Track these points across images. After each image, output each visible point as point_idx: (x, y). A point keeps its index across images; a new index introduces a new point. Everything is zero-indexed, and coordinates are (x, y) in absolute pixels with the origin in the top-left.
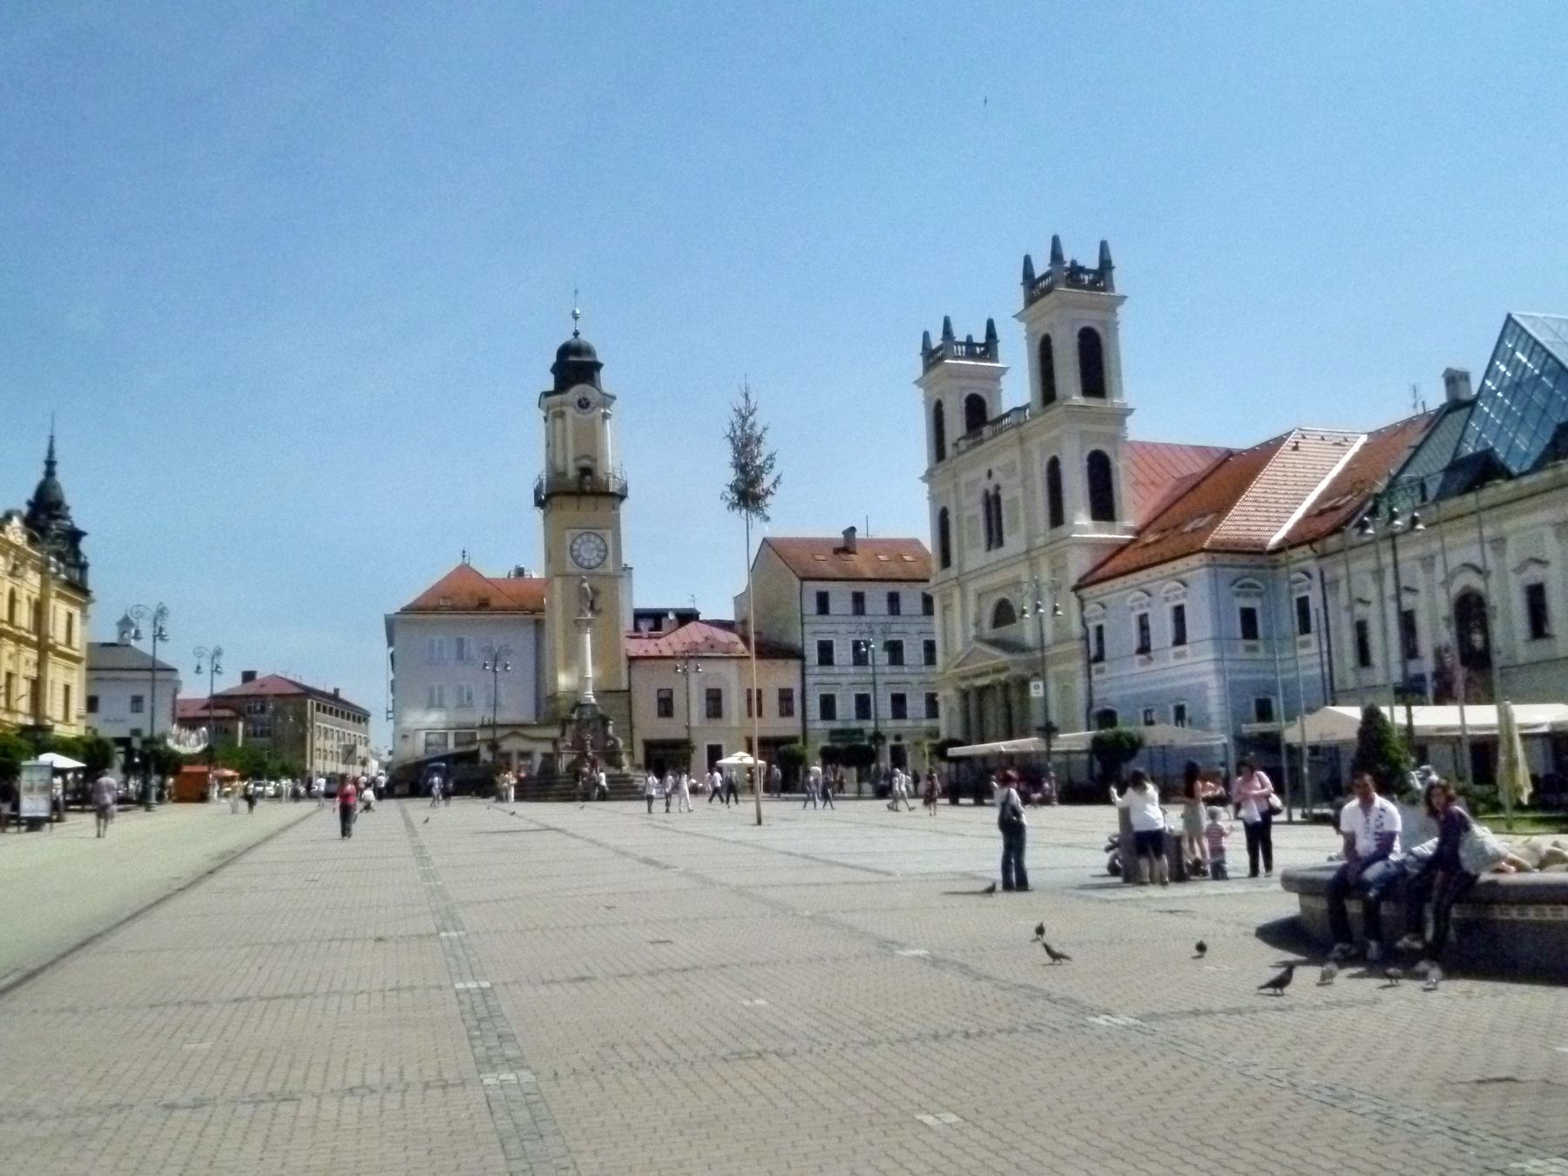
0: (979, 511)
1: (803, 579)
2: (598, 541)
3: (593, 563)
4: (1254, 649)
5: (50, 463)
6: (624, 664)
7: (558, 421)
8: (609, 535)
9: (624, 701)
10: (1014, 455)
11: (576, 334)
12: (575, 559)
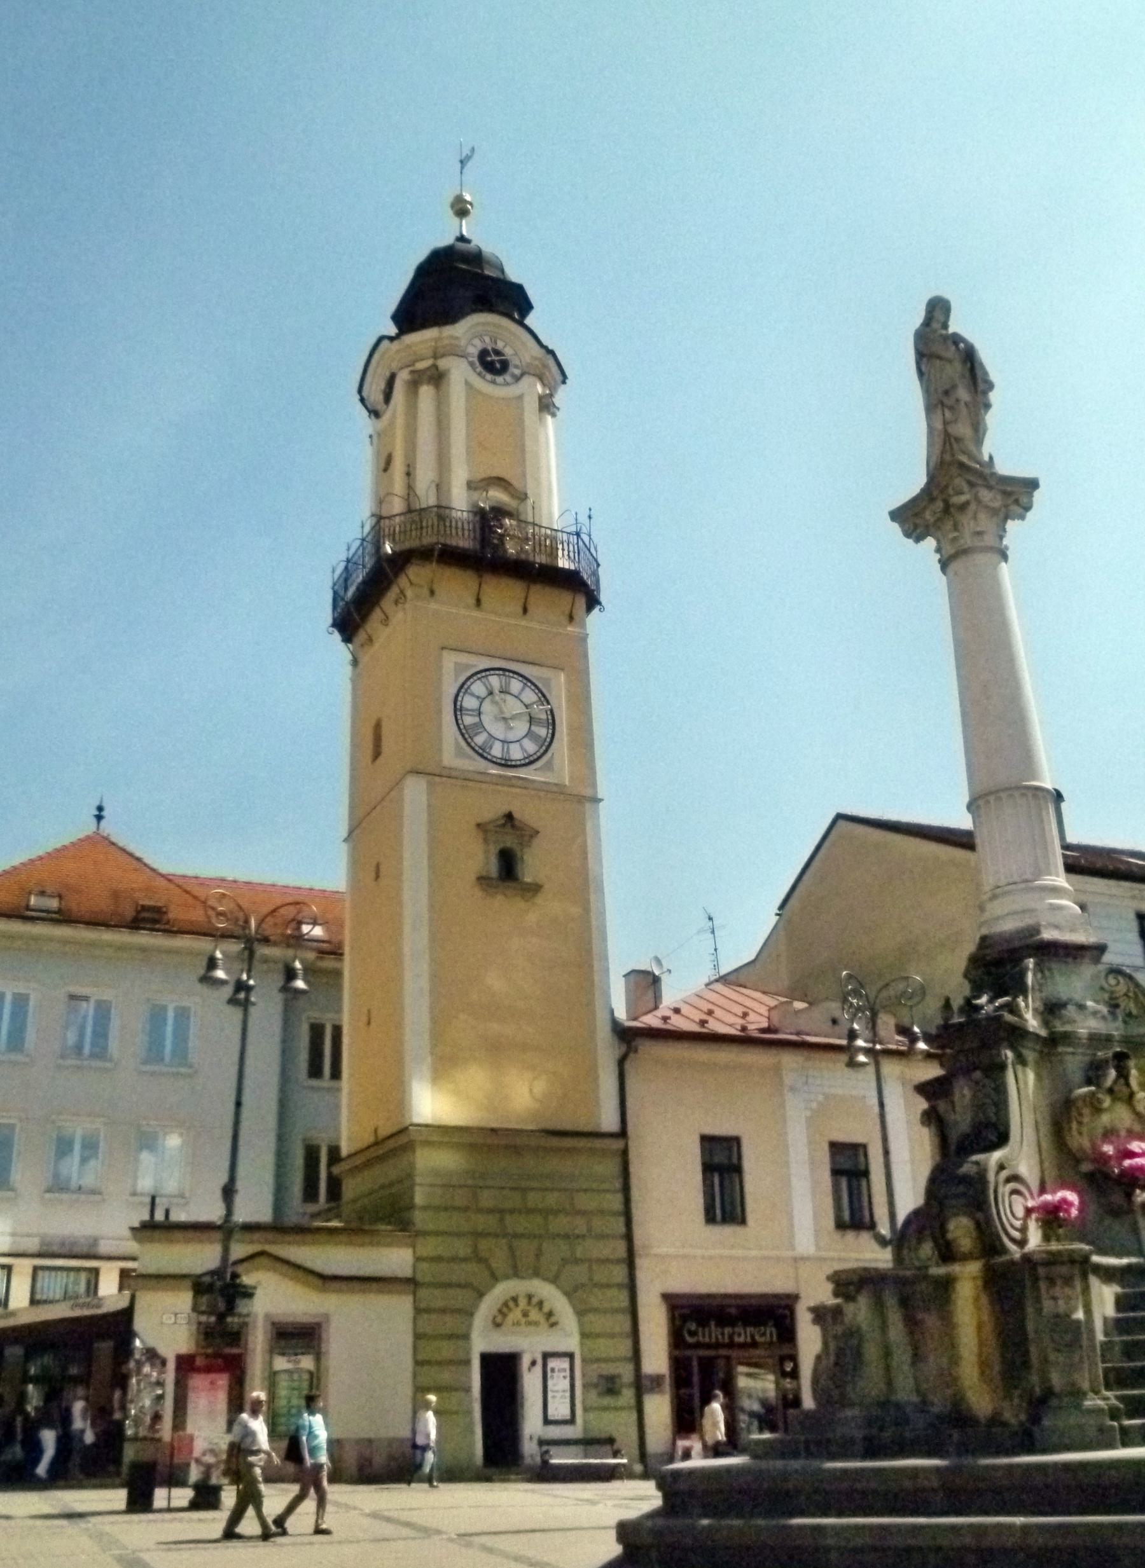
2: (530, 696)
3: (516, 754)
6: (606, 1052)
7: (426, 392)
8: (559, 686)
9: (609, 1168)
12: (466, 733)
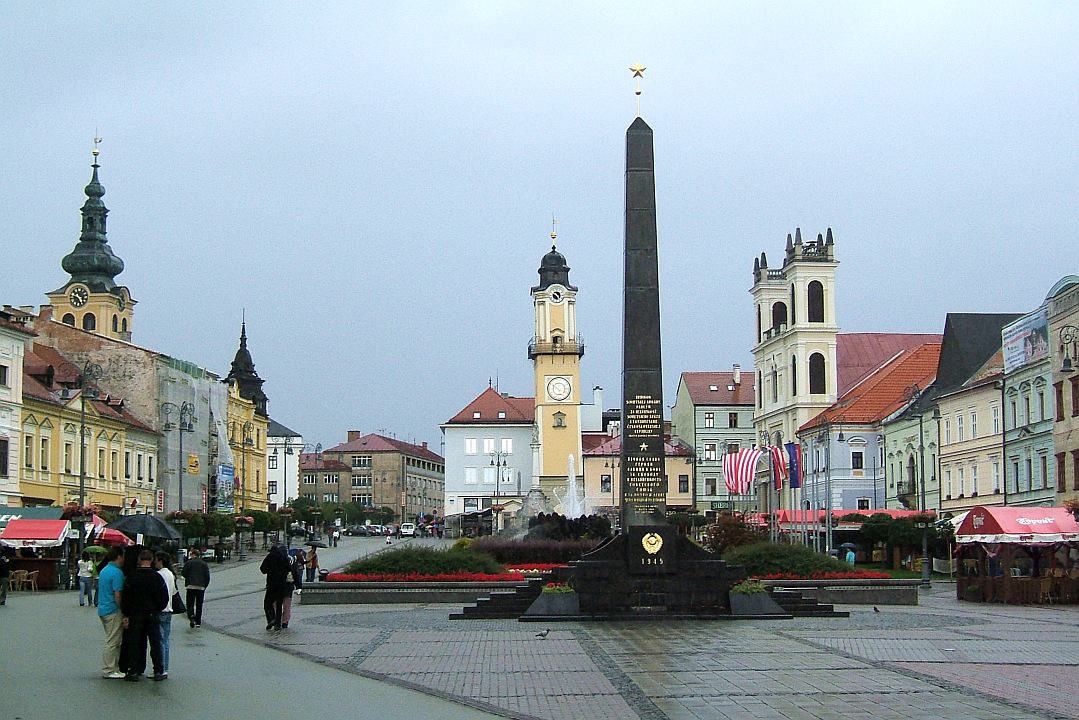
0: (770, 377)
1: (695, 405)
4: (861, 474)
5: (243, 339)
7: (541, 307)
10: (782, 350)
11: (554, 248)
